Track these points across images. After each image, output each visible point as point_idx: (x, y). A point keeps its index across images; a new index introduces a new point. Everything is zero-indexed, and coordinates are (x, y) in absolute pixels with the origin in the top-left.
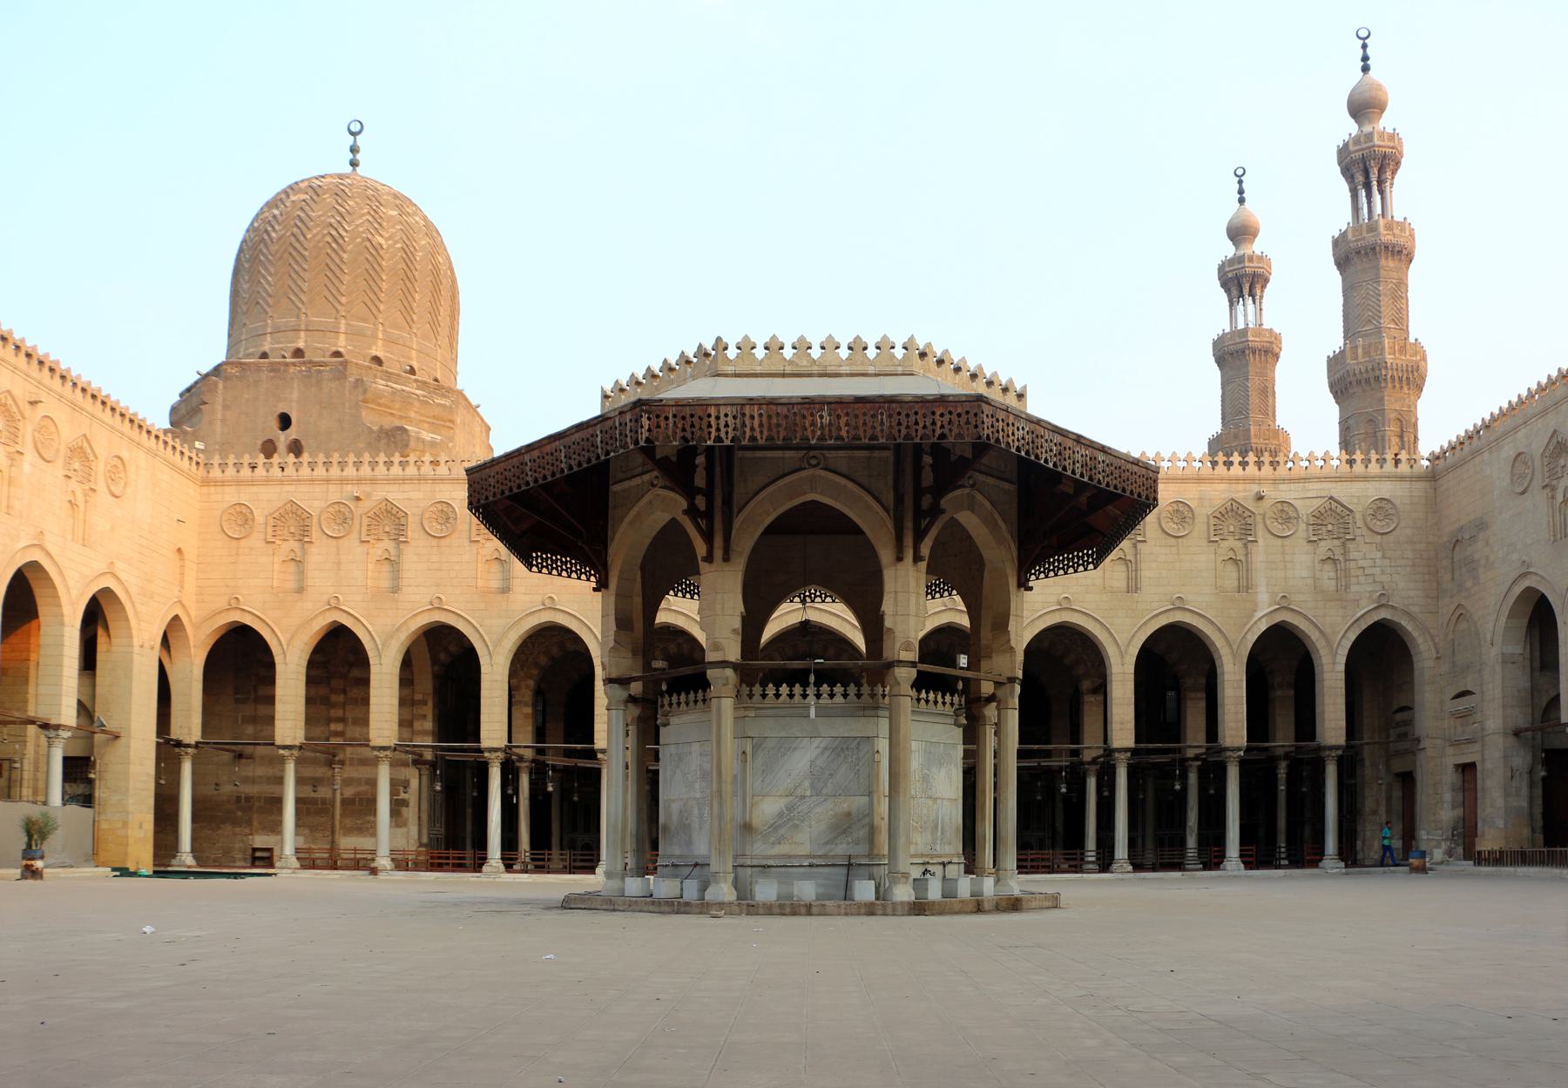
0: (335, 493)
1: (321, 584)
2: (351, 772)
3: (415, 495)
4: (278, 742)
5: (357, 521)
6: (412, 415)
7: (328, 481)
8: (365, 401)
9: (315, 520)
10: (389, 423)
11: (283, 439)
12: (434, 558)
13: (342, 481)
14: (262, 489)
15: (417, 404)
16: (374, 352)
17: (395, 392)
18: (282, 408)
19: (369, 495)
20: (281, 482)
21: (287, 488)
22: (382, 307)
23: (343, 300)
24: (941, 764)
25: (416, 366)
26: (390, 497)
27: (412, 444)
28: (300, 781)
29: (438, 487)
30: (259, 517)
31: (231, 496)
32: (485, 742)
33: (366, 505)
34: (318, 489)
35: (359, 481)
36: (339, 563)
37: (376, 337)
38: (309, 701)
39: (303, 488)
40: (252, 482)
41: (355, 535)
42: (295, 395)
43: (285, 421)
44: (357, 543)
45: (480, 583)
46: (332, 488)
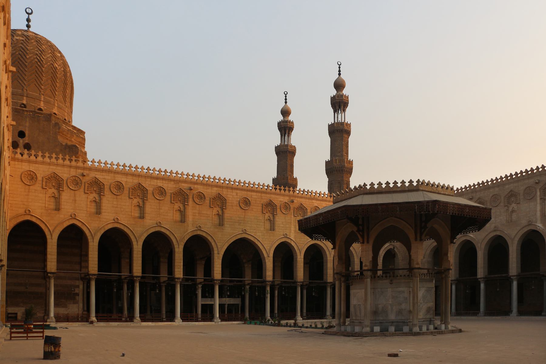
0: (73, 172)
1: (67, 207)
3: (107, 177)
5: (83, 185)
7: (70, 167)
9: (65, 182)
10: (69, 143)
11: (21, 142)
12: (115, 203)
13: (77, 168)
14: (41, 166)
15: (75, 136)
18: (21, 128)
19: (88, 175)
20: (49, 164)
21: (51, 167)
22: (57, 93)
23: (43, 87)
25: (66, 118)
26: (97, 176)
27: (79, 153)
29: (116, 175)
30: (40, 178)
31: (26, 167)
33: (87, 179)
34: (66, 169)
35: (84, 169)
39: (59, 168)
40: (36, 162)
41: (82, 190)
42: (27, 124)
43: (22, 134)
44: (83, 193)
46: (72, 170)
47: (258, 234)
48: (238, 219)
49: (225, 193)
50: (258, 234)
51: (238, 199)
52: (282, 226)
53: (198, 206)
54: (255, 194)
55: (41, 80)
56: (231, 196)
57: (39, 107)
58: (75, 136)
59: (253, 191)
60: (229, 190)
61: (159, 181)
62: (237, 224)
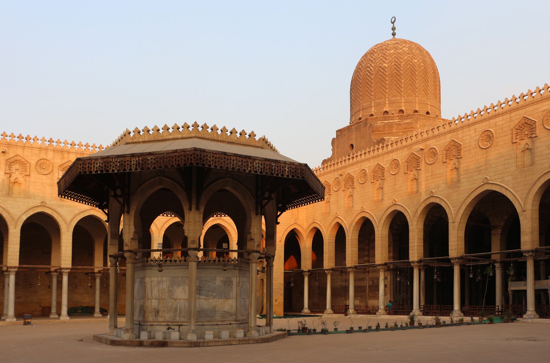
2: (371, 275)
4: (499, 255)
6: (394, 131)
8: (373, 132)
15: (395, 126)
16: (385, 110)
17: (385, 124)
28: (355, 280)
32: (411, 259)
33: (344, 176)
36: (338, 200)
37: (385, 103)
38: (360, 250)
45: (375, 198)
51: (478, 137)
53: (430, 166)
54: (501, 118)
55: (370, 88)
56: (468, 137)
58: (395, 126)
59: (498, 115)
60: (465, 130)
61: (394, 154)
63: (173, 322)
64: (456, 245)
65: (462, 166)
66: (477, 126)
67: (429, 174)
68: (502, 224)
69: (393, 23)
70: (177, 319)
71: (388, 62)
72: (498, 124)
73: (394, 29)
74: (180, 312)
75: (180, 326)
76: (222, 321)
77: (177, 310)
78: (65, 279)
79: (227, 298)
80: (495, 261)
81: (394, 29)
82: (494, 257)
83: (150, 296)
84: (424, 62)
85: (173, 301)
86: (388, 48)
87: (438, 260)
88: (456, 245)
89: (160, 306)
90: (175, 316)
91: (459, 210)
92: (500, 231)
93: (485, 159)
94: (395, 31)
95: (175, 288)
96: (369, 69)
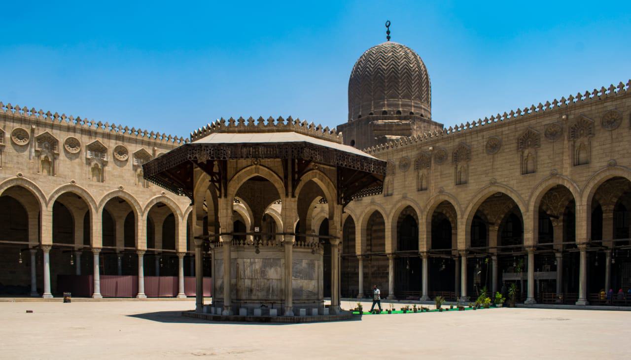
18: (352, 138)
24: (271, 267)
47: (512, 182)
48: (484, 169)
49: (468, 141)
50: (512, 182)
51: (485, 143)
52: (548, 161)
54: (506, 128)
57: (370, 112)
60: (473, 136)
62: (484, 176)
63: (266, 300)
64: (461, 240)
65: (471, 168)
66: (485, 133)
67: (439, 174)
68: (499, 222)
69: (388, 27)
70: (270, 297)
71: (386, 64)
72: (504, 133)
73: (388, 32)
74: (273, 291)
75: (272, 304)
76: (308, 300)
77: (269, 289)
78: (47, 256)
79: (311, 279)
80: (492, 254)
81: (388, 32)
82: (491, 251)
83: (242, 276)
84: (419, 67)
85: (266, 281)
86: (386, 51)
87: (409, 253)
88: (461, 240)
89: (253, 285)
90: (268, 295)
91: (467, 207)
92: (497, 228)
93: (491, 164)
94: (390, 35)
95: (267, 269)
96: (368, 70)
